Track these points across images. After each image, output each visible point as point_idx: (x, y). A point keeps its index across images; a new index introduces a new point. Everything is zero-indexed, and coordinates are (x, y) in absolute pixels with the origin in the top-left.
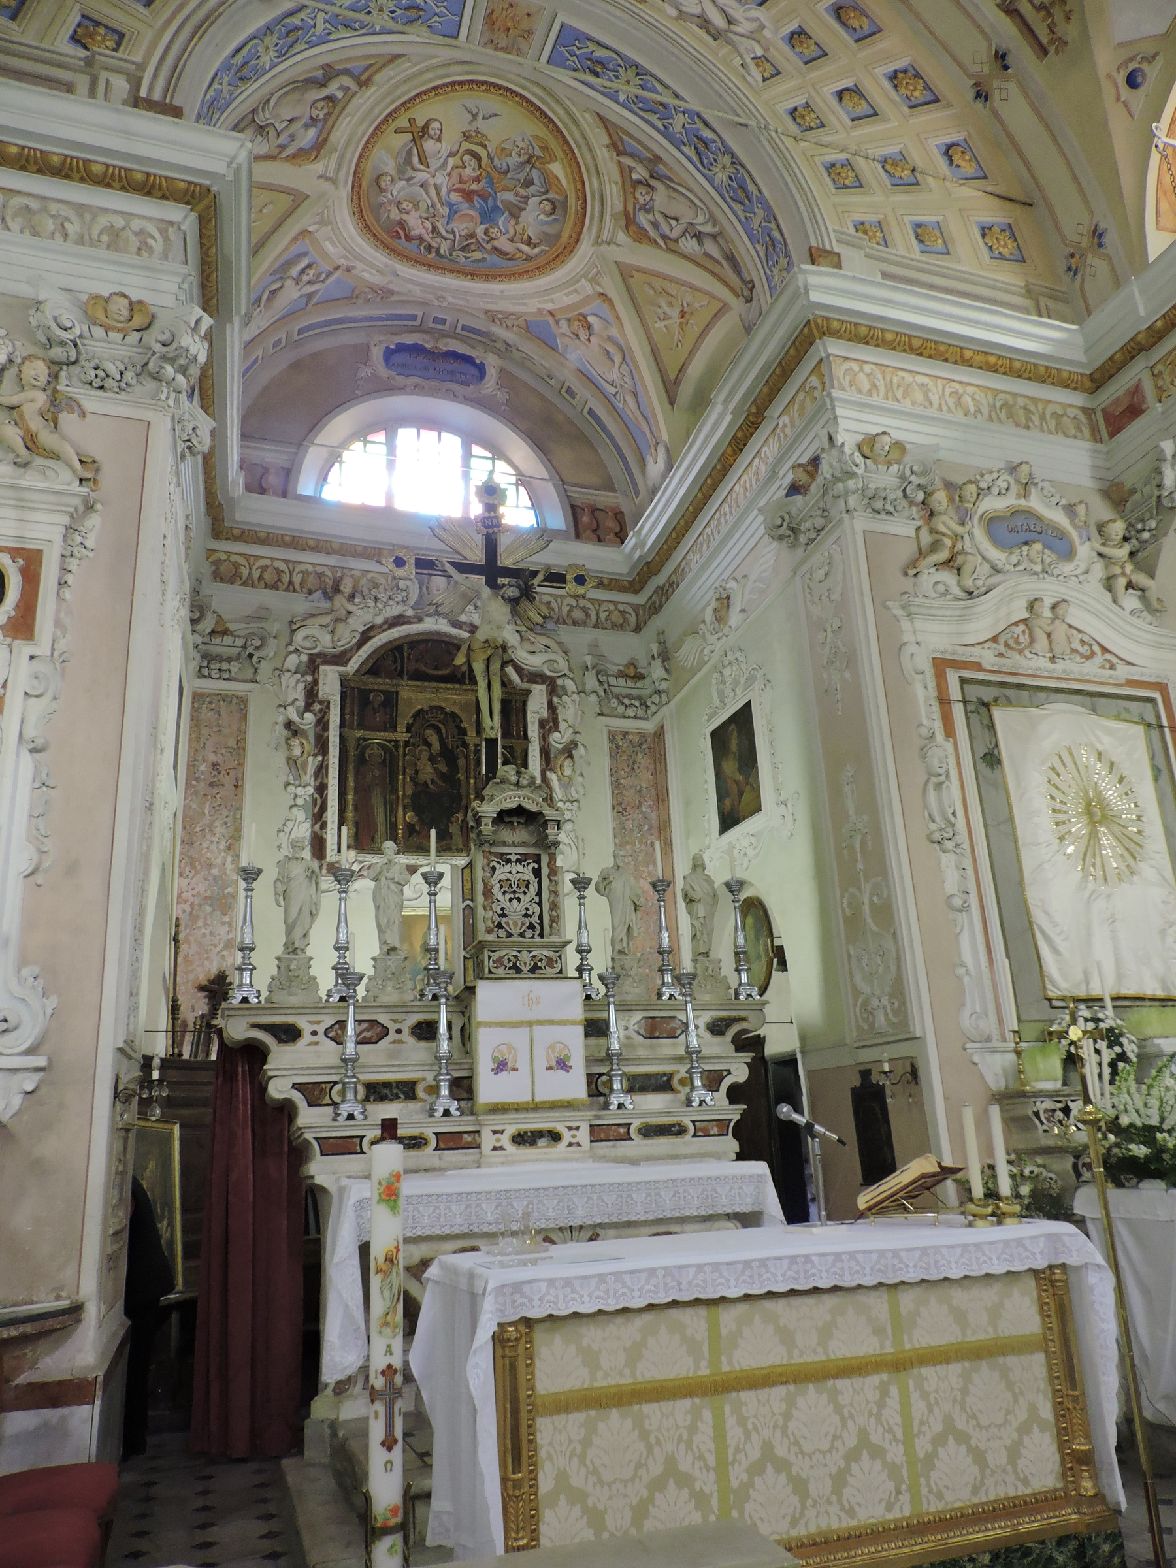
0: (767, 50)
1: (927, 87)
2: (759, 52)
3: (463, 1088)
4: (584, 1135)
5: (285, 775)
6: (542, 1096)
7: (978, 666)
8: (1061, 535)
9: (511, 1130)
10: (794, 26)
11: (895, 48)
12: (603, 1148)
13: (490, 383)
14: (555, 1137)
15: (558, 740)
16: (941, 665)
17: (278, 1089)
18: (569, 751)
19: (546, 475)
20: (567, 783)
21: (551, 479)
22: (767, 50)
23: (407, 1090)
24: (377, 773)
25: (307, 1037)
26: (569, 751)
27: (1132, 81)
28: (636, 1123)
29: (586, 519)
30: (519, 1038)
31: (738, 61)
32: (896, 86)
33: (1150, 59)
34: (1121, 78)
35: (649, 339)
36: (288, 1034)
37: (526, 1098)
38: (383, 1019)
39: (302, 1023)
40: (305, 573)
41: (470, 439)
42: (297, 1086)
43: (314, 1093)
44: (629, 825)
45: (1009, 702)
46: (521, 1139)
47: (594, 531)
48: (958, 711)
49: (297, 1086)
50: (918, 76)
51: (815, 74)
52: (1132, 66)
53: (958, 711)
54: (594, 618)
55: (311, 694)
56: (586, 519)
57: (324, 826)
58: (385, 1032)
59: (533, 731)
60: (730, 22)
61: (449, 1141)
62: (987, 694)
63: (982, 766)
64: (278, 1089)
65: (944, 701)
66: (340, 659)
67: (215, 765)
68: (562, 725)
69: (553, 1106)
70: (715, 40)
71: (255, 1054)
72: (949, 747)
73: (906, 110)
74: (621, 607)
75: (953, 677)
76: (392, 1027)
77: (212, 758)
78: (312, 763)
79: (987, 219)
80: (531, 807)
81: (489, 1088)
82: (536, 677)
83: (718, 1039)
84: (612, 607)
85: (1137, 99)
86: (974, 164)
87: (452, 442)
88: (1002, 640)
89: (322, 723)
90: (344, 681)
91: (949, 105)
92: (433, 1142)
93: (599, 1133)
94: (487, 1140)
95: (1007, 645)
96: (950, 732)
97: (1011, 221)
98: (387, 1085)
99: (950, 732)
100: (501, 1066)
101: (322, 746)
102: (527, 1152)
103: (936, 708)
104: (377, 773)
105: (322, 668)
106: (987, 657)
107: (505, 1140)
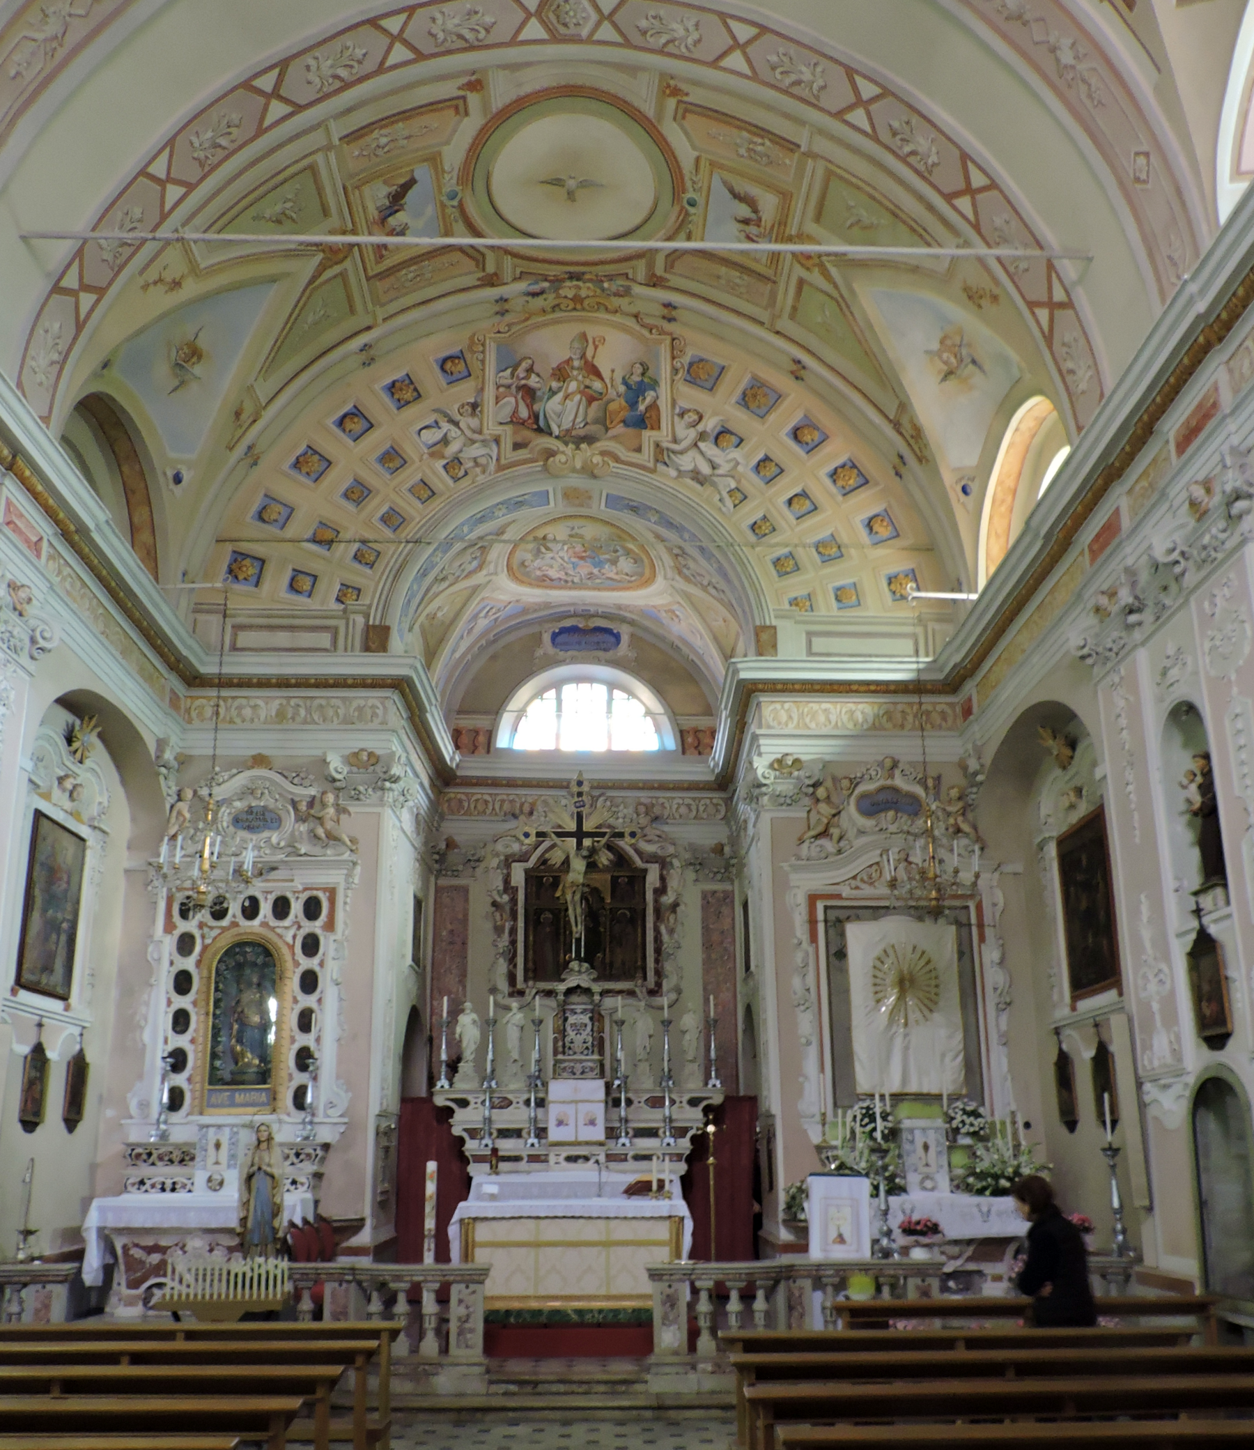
0: (738, 482)
1: (860, 474)
2: (733, 485)
3: (541, 1133)
4: (602, 1158)
5: (493, 936)
6: (581, 1139)
7: (839, 897)
8: (914, 798)
9: (564, 1155)
10: (760, 456)
11: (836, 452)
12: (612, 1165)
13: (623, 649)
14: (586, 1159)
15: (668, 899)
16: (812, 899)
17: (457, 1131)
18: (675, 906)
19: (662, 711)
20: (671, 931)
21: (666, 713)
22: (738, 482)
23: (517, 1133)
24: (548, 930)
25: (472, 1106)
26: (675, 906)
27: (965, 490)
28: (631, 1154)
29: (690, 740)
30: (570, 1109)
31: (718, 497)
32: (834, 481)
33: (973, 479)
34: (959, 489)
35: (711, 631)
36: (463, 1103)
37: (573, 1139)
38: (510, 1096)
39: (470, 1098)
40: (503, 801)
41: (612, 686)
42: (465, 1130)
43: (473, 1133)
44: (713, 956)
45: (858, 918)
46: (569, 1159)
47: (696, 748)
48: (821, 927)
49: (465, 1130)
50: (854, 466)
51: (773, 490)
52: (963, 483)
53: (821, 927)
54: (694, 813)
55: (507, 881)
56: (690, 740)
57: (515, 966)
58: (511, 1103)
59: (650, 896)
60: (714, 468)
61: (534, 1159)
62: (842, 914)
63: (832, 959)
64: (457, 1131)
65: (812, 922)
66: (523, 858)
67: (452, 931)
68: (670, 892)
69: (587, 1143)
70: (702, 485)
71: (449, 1112)
72: (811, 950)
73: (840, 498)
74: (715, 801)
75: (820, 906)
76: (515, 1101)
77: (450, 927)
78: (508, 926)
79: (893, 570)
80: (584, 985)
81: (554, 1134)
82: (653, 858)
83: (694, 1109)
84: (708, 801)
85: (970, 501)
86: (890, 528)
87: (601, 689)
88: (859, 878)
89: (514, 901)
90: (527, 871)
91: (877, 484)
92: (526, 1159)
93: (610, 1158)
94: (552, 1159)
95: (862, 880)
96: (813, 938)
97: (911, 566)
98: (508, 1130)
99: (813, 938)
100: (560, 1123)
101: (514, 916)
102: (572, 1165)
103: (807, 927)
104: (548, 930)
105: (514, 865)
106: (846, 891)
107: (561, 1159)
